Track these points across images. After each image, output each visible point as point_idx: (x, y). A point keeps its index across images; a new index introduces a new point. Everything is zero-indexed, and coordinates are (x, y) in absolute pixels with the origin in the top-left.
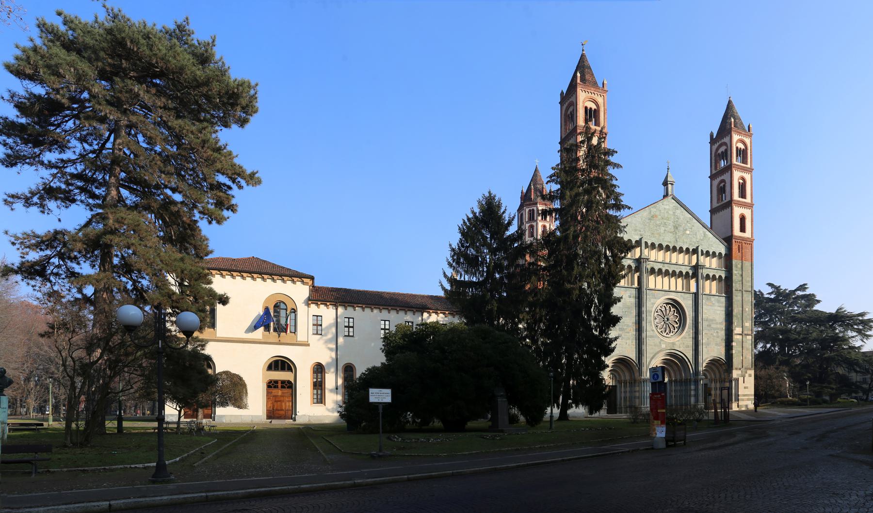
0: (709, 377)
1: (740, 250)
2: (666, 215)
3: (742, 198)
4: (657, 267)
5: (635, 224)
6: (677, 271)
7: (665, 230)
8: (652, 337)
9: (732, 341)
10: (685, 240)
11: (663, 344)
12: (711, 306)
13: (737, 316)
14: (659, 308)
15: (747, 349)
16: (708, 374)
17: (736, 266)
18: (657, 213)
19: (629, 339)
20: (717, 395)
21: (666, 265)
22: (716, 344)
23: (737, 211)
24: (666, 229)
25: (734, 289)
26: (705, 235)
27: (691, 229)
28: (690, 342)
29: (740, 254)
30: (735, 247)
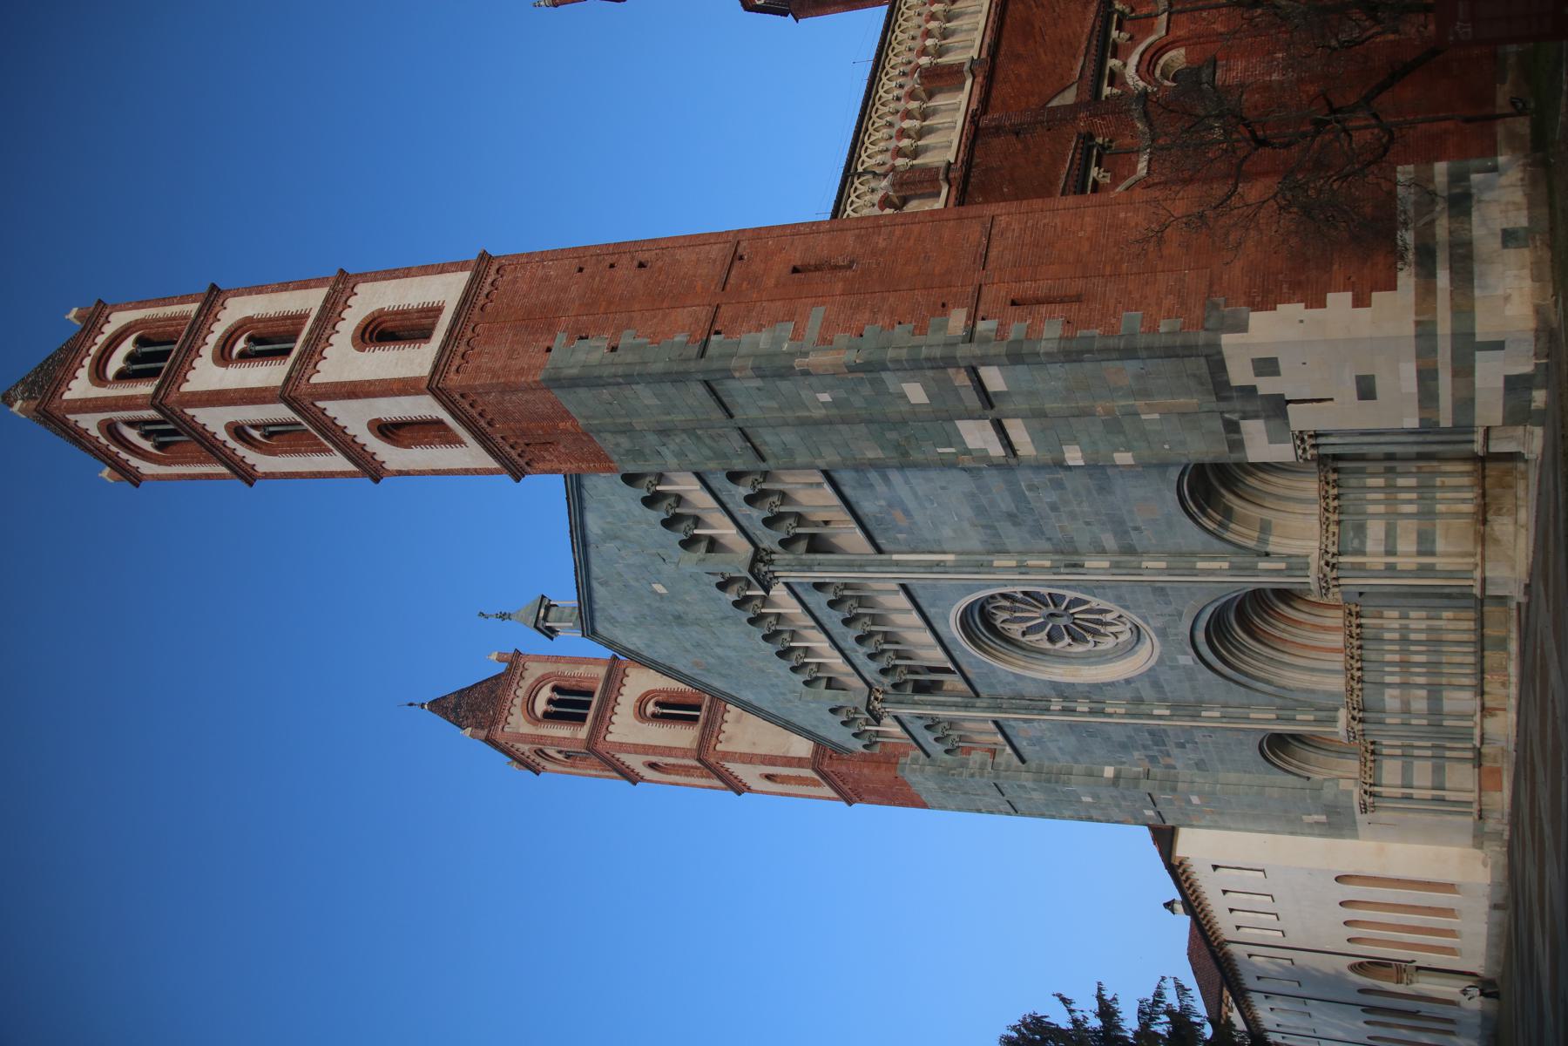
7: (719, 646)
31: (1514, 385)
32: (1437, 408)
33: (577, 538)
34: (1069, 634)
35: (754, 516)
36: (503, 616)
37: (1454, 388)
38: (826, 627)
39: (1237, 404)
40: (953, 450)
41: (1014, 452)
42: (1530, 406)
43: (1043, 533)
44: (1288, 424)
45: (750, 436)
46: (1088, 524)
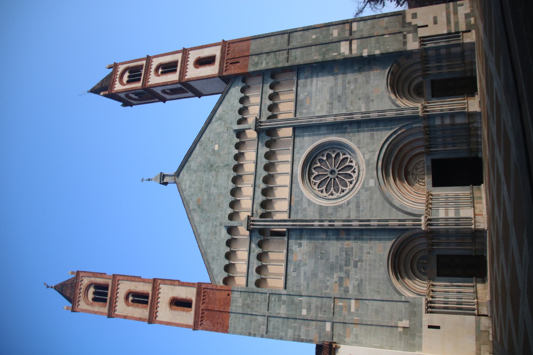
0: (420, 79)
1: (236, 60)
2: (197, 184)
3: (176, 66)
4: (260, 198)
5: (209, 234)
6: (265, 161)
7: (214, 185)
8: (358, 206)
9: (362, 57)
10: (226, 152)
11: (368, 184)
12: (311, 99)
13: (324, 54)
14: (316, 187)
15: (373, 27)
16: (416, 82)
17: (256, 64)
18: (195, 199)
19: (361, 248)
20: (448, 65)
21: (257, 183)
22: (367, 82)
23: (192, 72)
24: (213, 183)
25: (287, 65)
26: (220, 119)
27: (212, 142)
28: (364, 136)
29: (241, 60)
30: (233, 70)
31: (467, 16)
32: (451, 26)
33: (210, 117)
34: (333, 187)
35: (268, 102)
36: (149, 180)
37: (454, 19)
38: (257, 170)
39: (406, 29)
40: (336, 54)
41: (351, 52)
42: (470, 23)
43: (345, 105)
44: (417, 34)
45: (289, 53)
46: (359, 99)
